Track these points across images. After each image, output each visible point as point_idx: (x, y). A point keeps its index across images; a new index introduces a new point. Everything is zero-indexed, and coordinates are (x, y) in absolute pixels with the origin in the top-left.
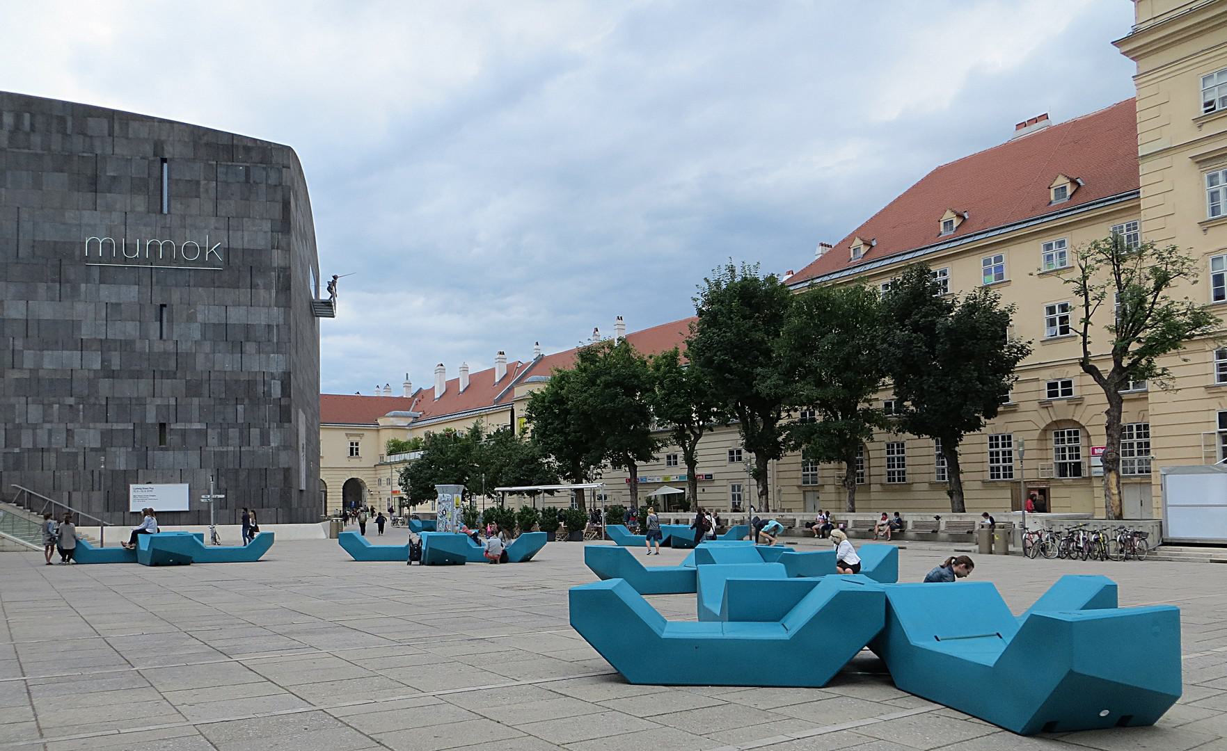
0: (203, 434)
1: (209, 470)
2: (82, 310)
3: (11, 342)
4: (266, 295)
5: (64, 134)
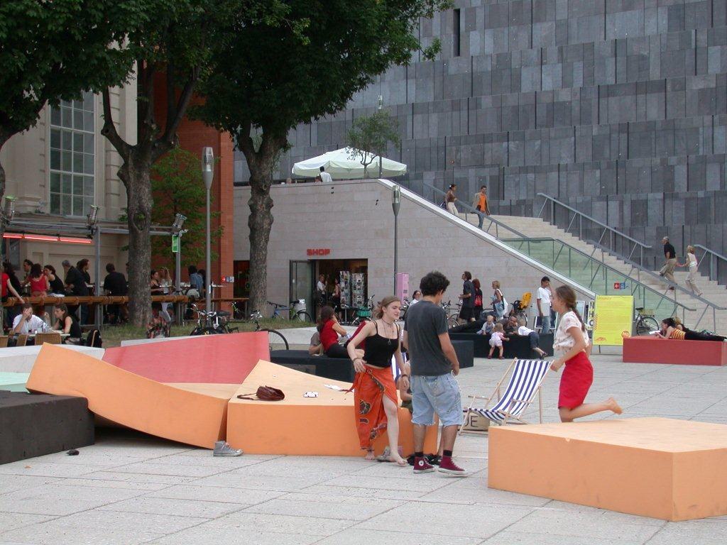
3: (693, 38)
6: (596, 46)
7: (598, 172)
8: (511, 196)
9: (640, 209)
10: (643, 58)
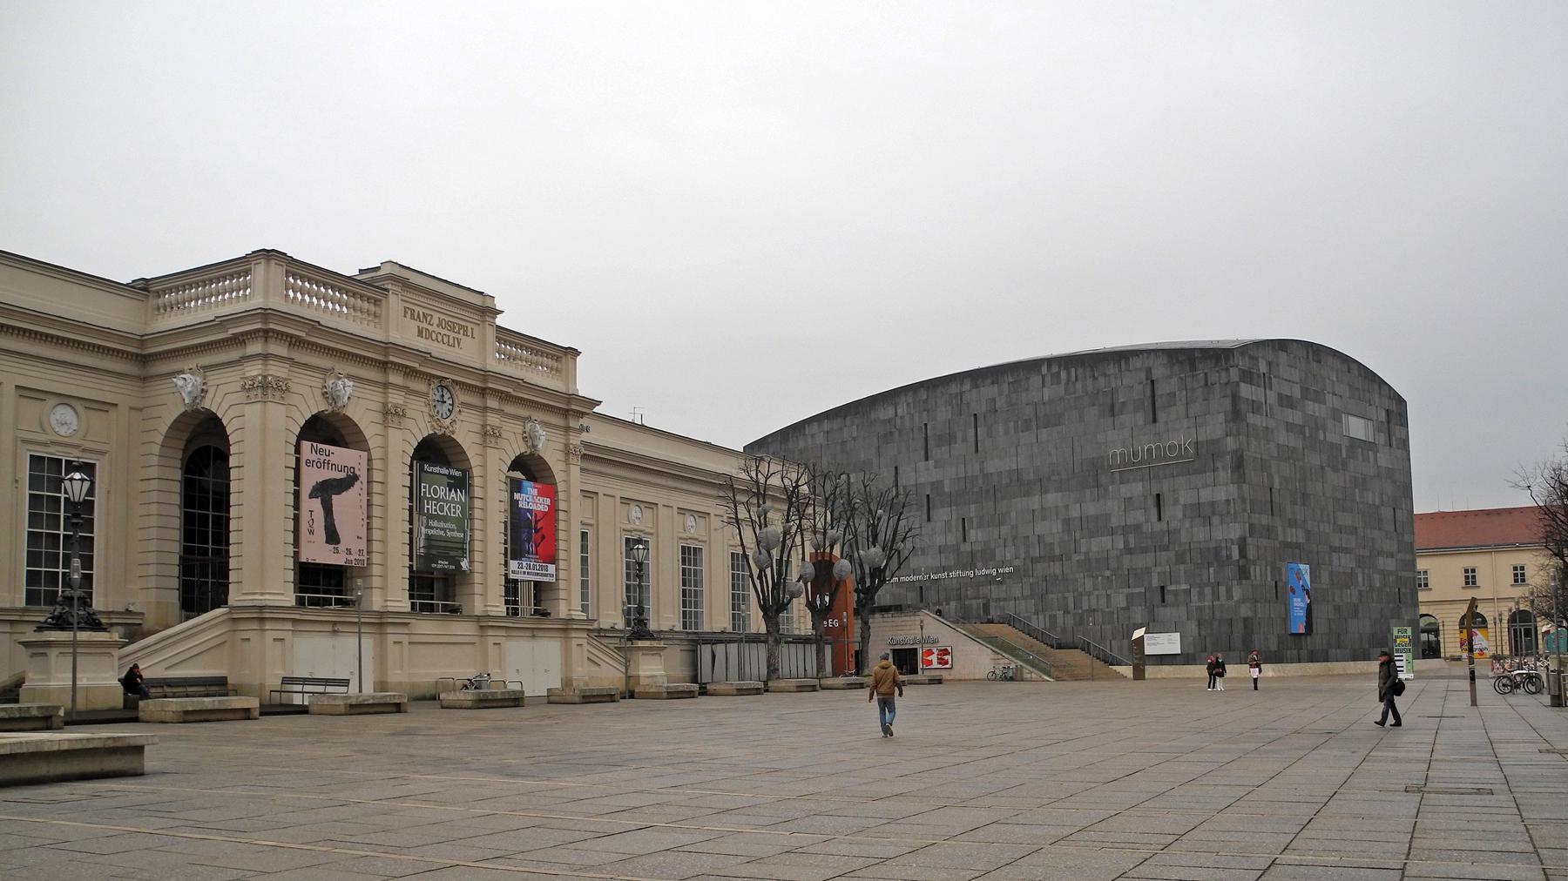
0: (1188, 593)
1: (1193, 621)
2: (1112, 506)
4: (1225, 475)
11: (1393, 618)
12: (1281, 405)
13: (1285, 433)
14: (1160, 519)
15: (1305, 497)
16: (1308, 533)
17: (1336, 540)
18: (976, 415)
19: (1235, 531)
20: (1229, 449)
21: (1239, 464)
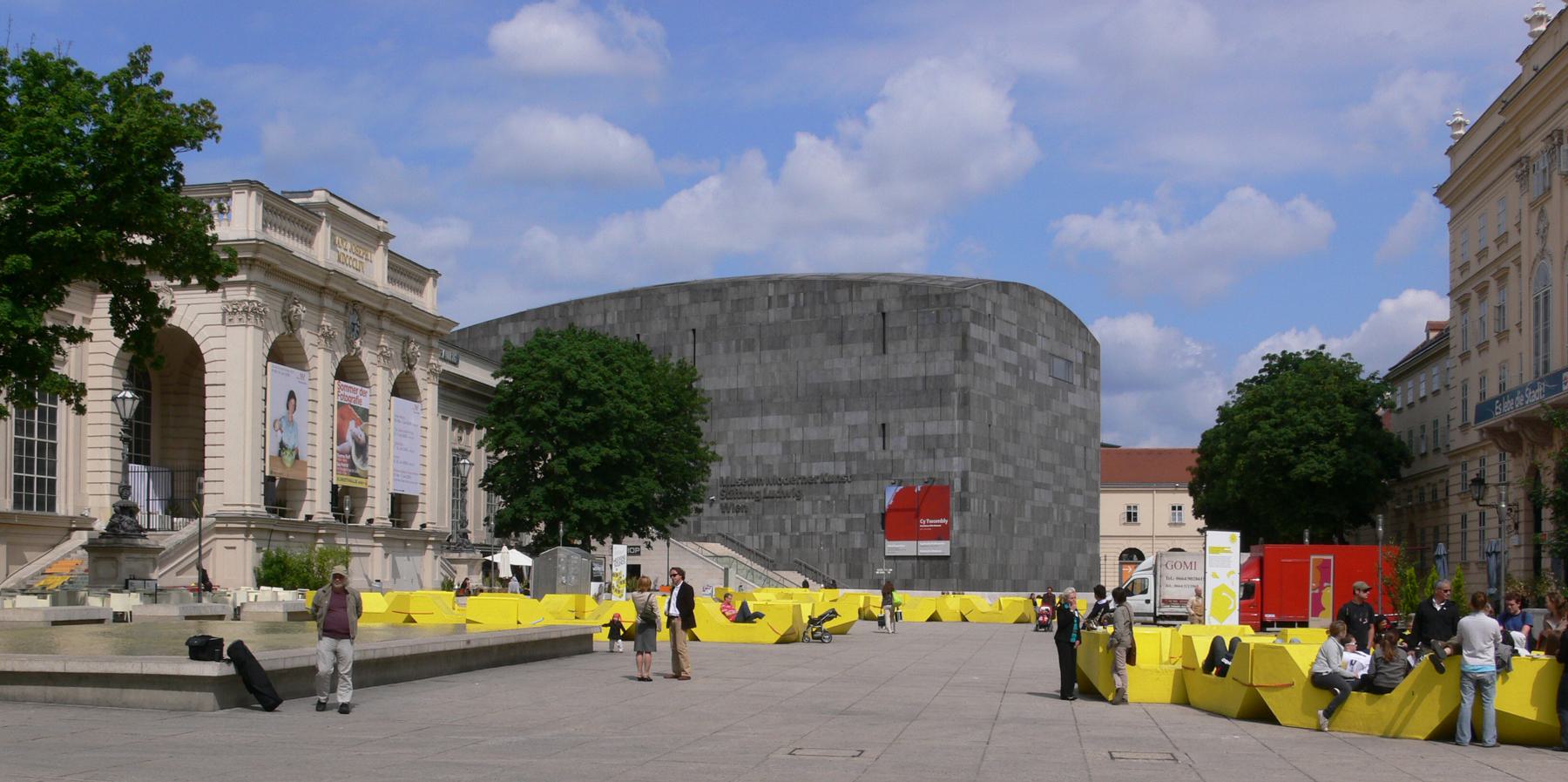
2: (836, 434)
4: (954, 411)
5: (823, 303)
6: (748, 459)
7: (748, 521)
8: (704, 531)
9: (768, 540)
10: (769, 465)
11: (1078, 552)
12: (1001, 346)
13: (1003, 372)
14: (884, 448)
15: (1016, 433)
16: (1017, 468)
17: (1040, 476)
18: (694, 331)
19: (957, 465)
20: (957, 386)
21: (965, 401)
